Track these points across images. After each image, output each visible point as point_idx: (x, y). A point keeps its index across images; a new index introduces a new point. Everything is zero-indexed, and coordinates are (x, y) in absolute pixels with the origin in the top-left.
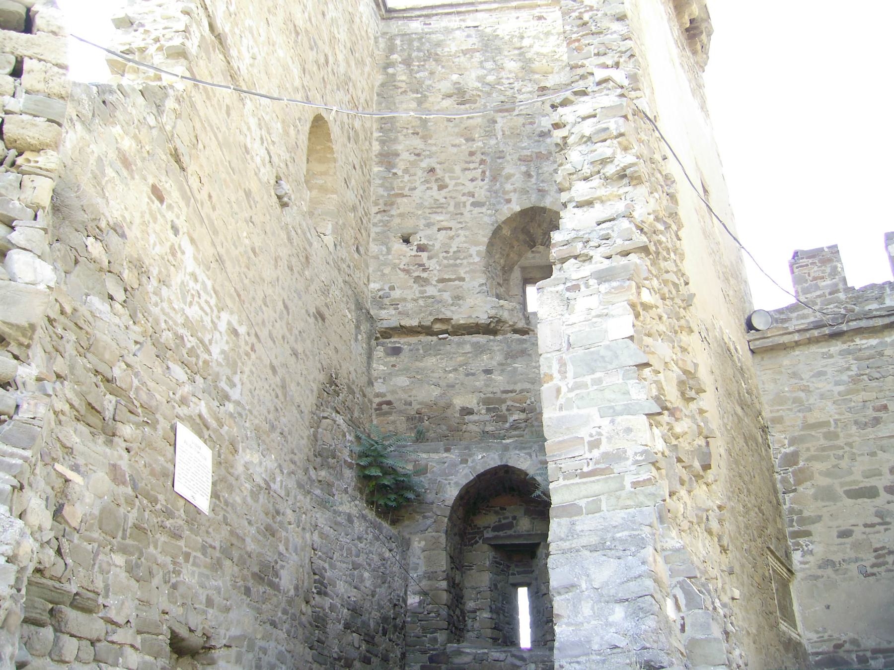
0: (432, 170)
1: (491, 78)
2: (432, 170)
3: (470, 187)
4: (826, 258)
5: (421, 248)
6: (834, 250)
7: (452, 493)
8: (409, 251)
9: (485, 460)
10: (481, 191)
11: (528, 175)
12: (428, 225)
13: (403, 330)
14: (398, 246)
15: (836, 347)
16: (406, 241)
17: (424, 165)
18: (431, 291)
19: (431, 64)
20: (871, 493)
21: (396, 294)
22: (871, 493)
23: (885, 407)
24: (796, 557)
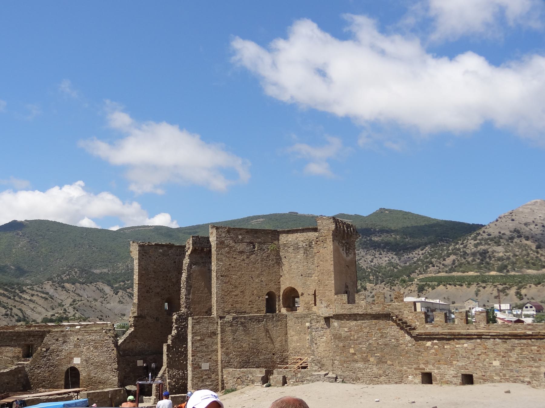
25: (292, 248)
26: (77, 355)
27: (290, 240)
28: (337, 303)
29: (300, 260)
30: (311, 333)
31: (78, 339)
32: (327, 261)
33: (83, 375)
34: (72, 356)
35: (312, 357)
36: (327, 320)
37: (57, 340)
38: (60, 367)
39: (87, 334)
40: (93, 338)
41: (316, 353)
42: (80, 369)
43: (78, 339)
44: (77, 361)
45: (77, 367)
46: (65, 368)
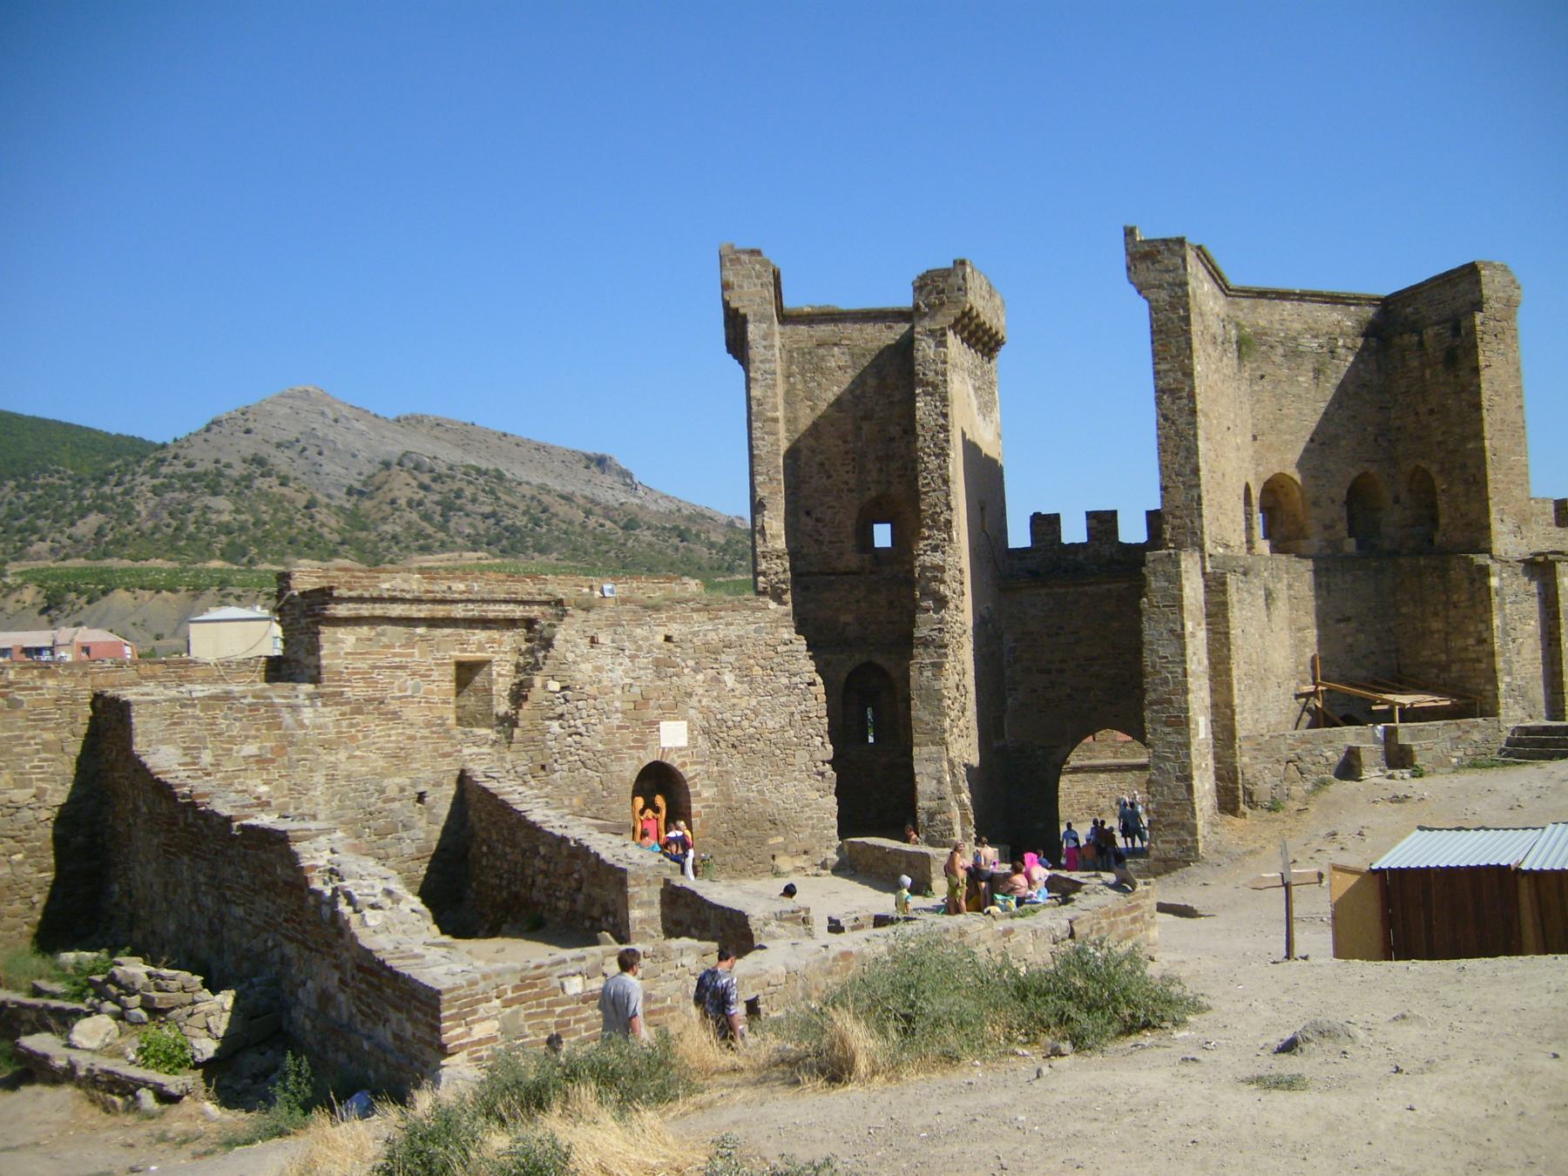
0: (822, 464)
1: (858, 392)
2: (822, 464)
3: (846, 477)
4: (1054, 520)
5: (818, 520)
6: (1057, 516)
7: (844, 675)
8: (810, 522)
9: (859, 658)
10: (853, 482)
11: (881, 470)
12: (822, 504)
13: (809, 574)
14: (804, 519)
15: (1044, 591)
16: (808, 513)
17: (817, 459)
18: (825, 548)
19: (818, 377)
20: (1048, 672)
21: (805, 551)
22: (1048, 672)
23: (1061, 628)
24: (1010, 700)
25: (1280, 350)
26: (673, 710)
27: (1262, 323)
28: (1537, 522)
29: (1307, 390)
30: (1501, 608)
31: (668, 639)
32: (1507, 396)
33: (703, 795)
34: (652, 713)
35: (1507, 679)
36: (1541, 569)
37: (593, 641)
38: (615, 767)
39: (703, 616)
40: (733, 633)
41: (1516, 666)
42: (688, 772)
43: (668, 639)
44: (672, 737)
45: (674, 761)
46: (630, 770)
